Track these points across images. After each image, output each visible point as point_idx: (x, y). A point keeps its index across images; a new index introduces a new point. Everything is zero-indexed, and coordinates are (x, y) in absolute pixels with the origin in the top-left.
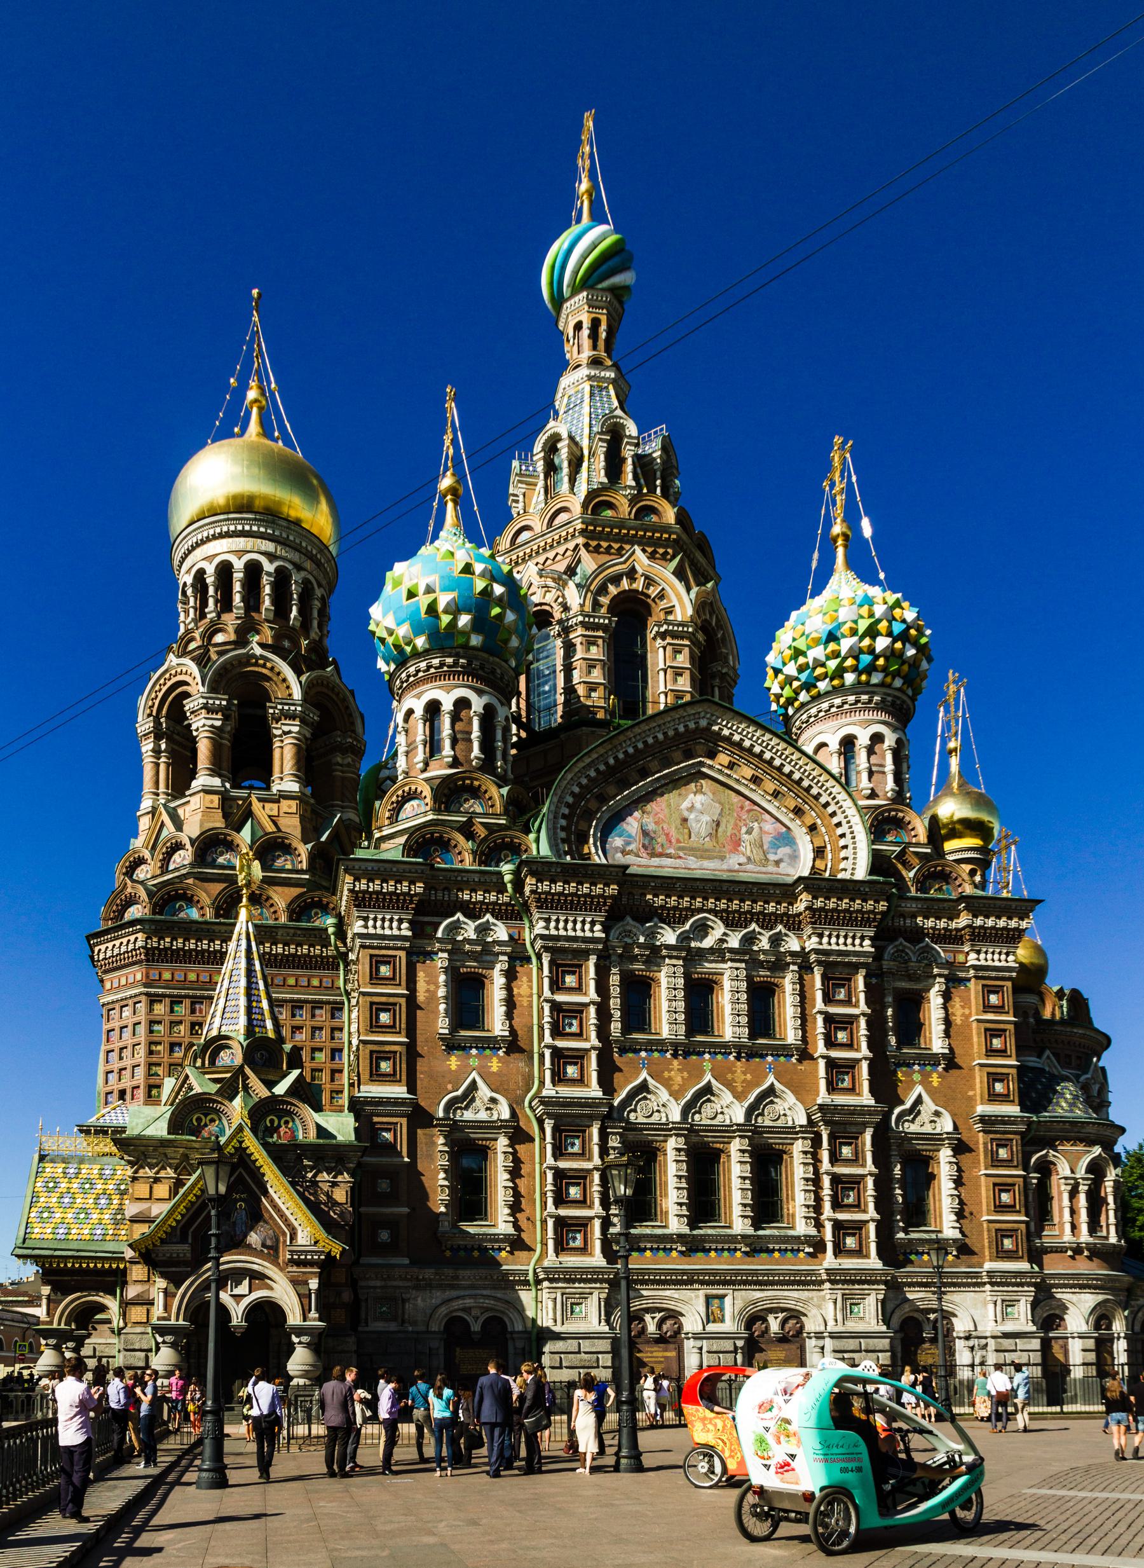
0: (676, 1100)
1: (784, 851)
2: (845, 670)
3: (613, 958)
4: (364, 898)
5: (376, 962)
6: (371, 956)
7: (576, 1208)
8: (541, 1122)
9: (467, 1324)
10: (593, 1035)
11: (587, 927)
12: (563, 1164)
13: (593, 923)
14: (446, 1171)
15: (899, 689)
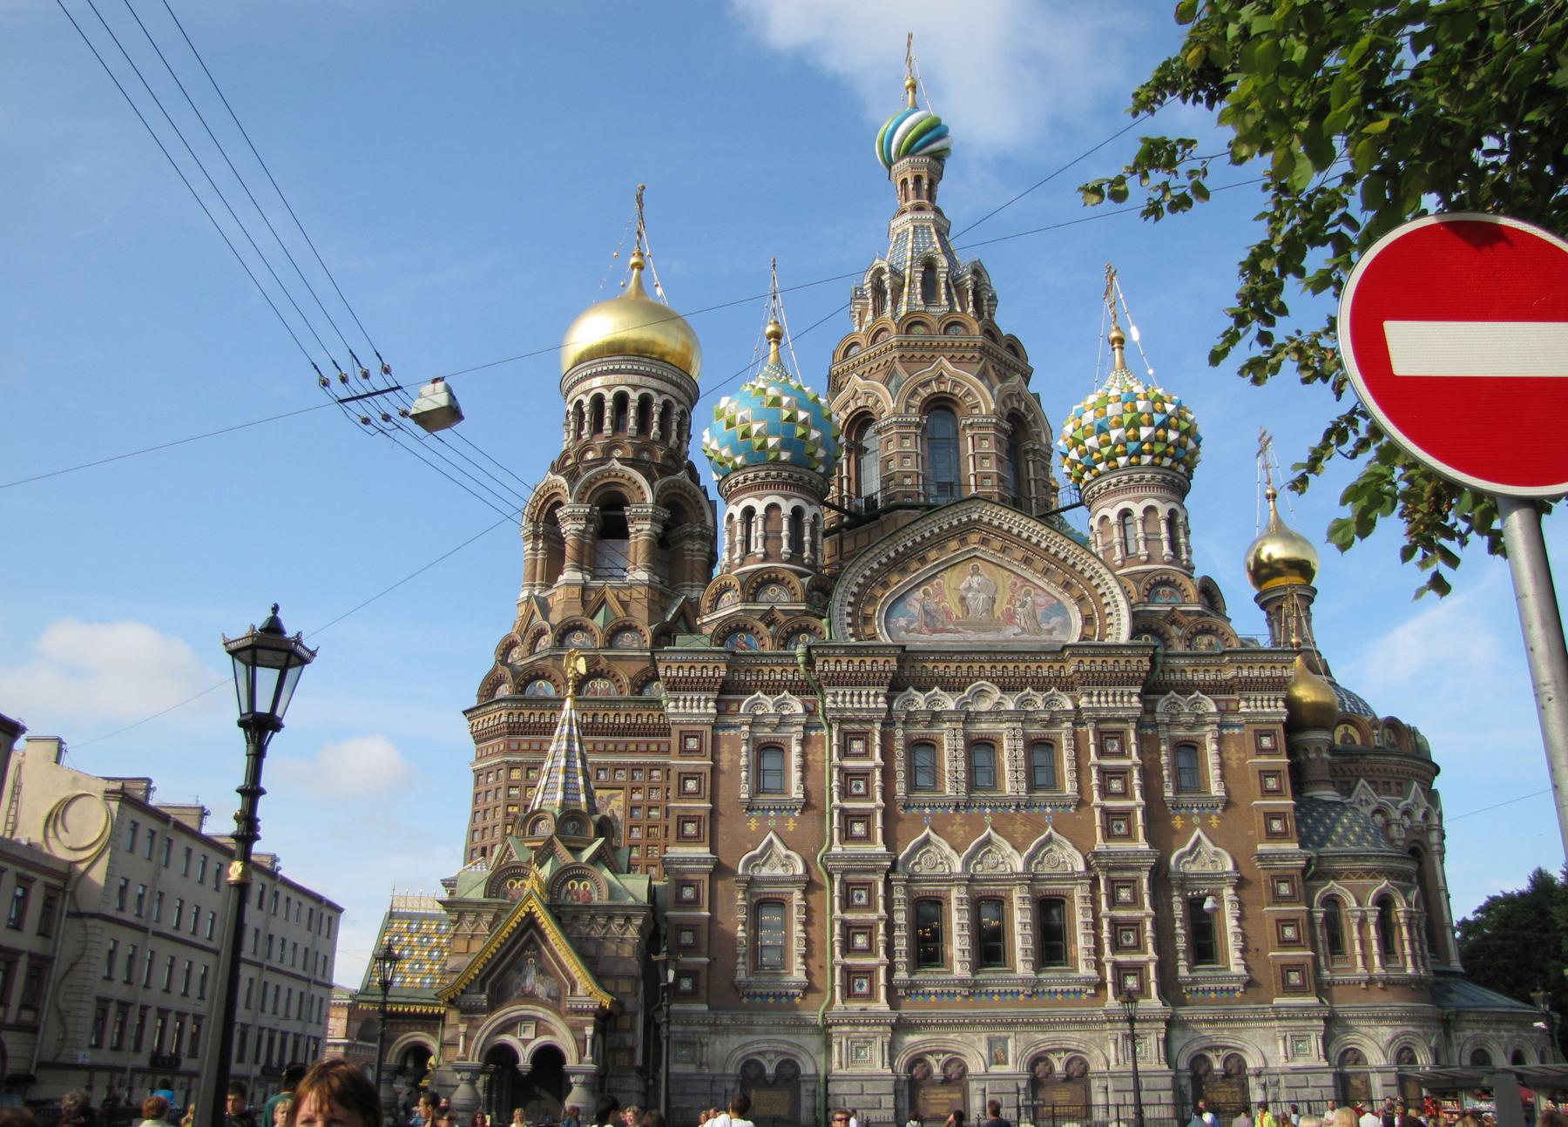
0: (958, 852)
1: (1055, 621)
2: (1118, 455)
3: (900, 725)
4: (674, 682)
5: (684, 736)
6: (681, 732)
7: (866, 957)
8: (831, 877)
9: (762, 1068)
10: (878, 795)
11: (871, 699)
12: (849, 916)
13: (876, 695)
14: (744, 924)
15: (1170, 468)
